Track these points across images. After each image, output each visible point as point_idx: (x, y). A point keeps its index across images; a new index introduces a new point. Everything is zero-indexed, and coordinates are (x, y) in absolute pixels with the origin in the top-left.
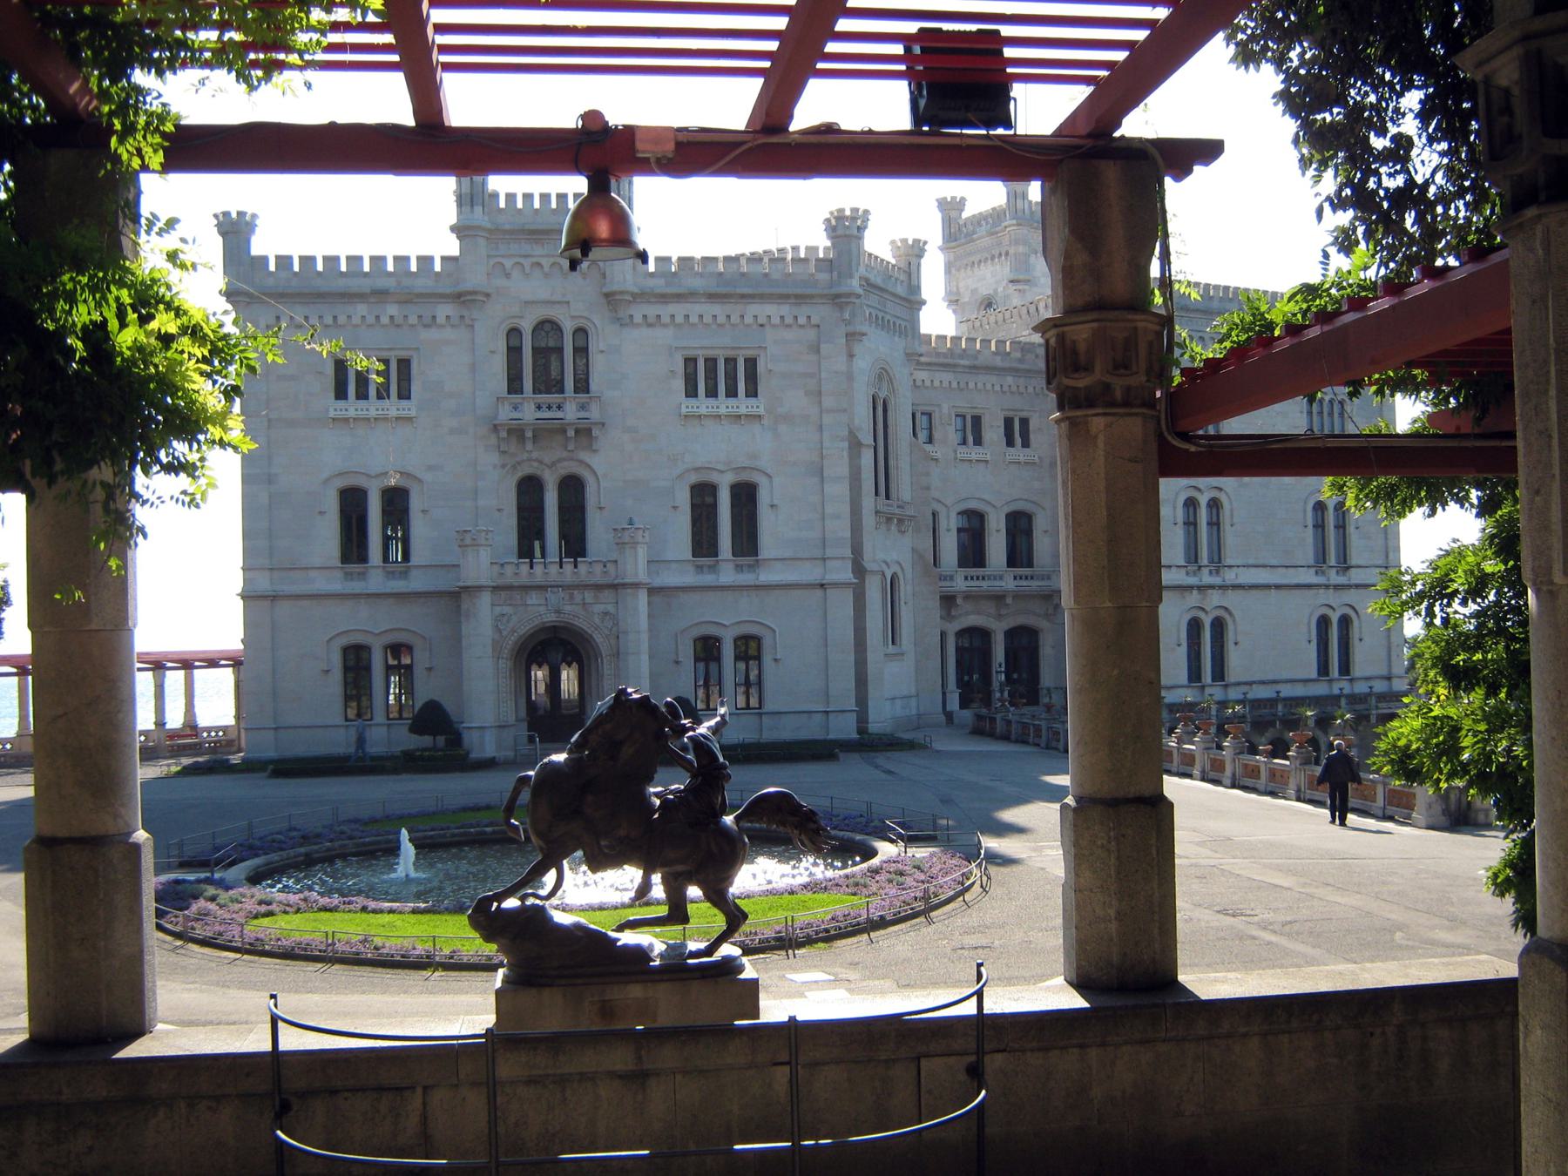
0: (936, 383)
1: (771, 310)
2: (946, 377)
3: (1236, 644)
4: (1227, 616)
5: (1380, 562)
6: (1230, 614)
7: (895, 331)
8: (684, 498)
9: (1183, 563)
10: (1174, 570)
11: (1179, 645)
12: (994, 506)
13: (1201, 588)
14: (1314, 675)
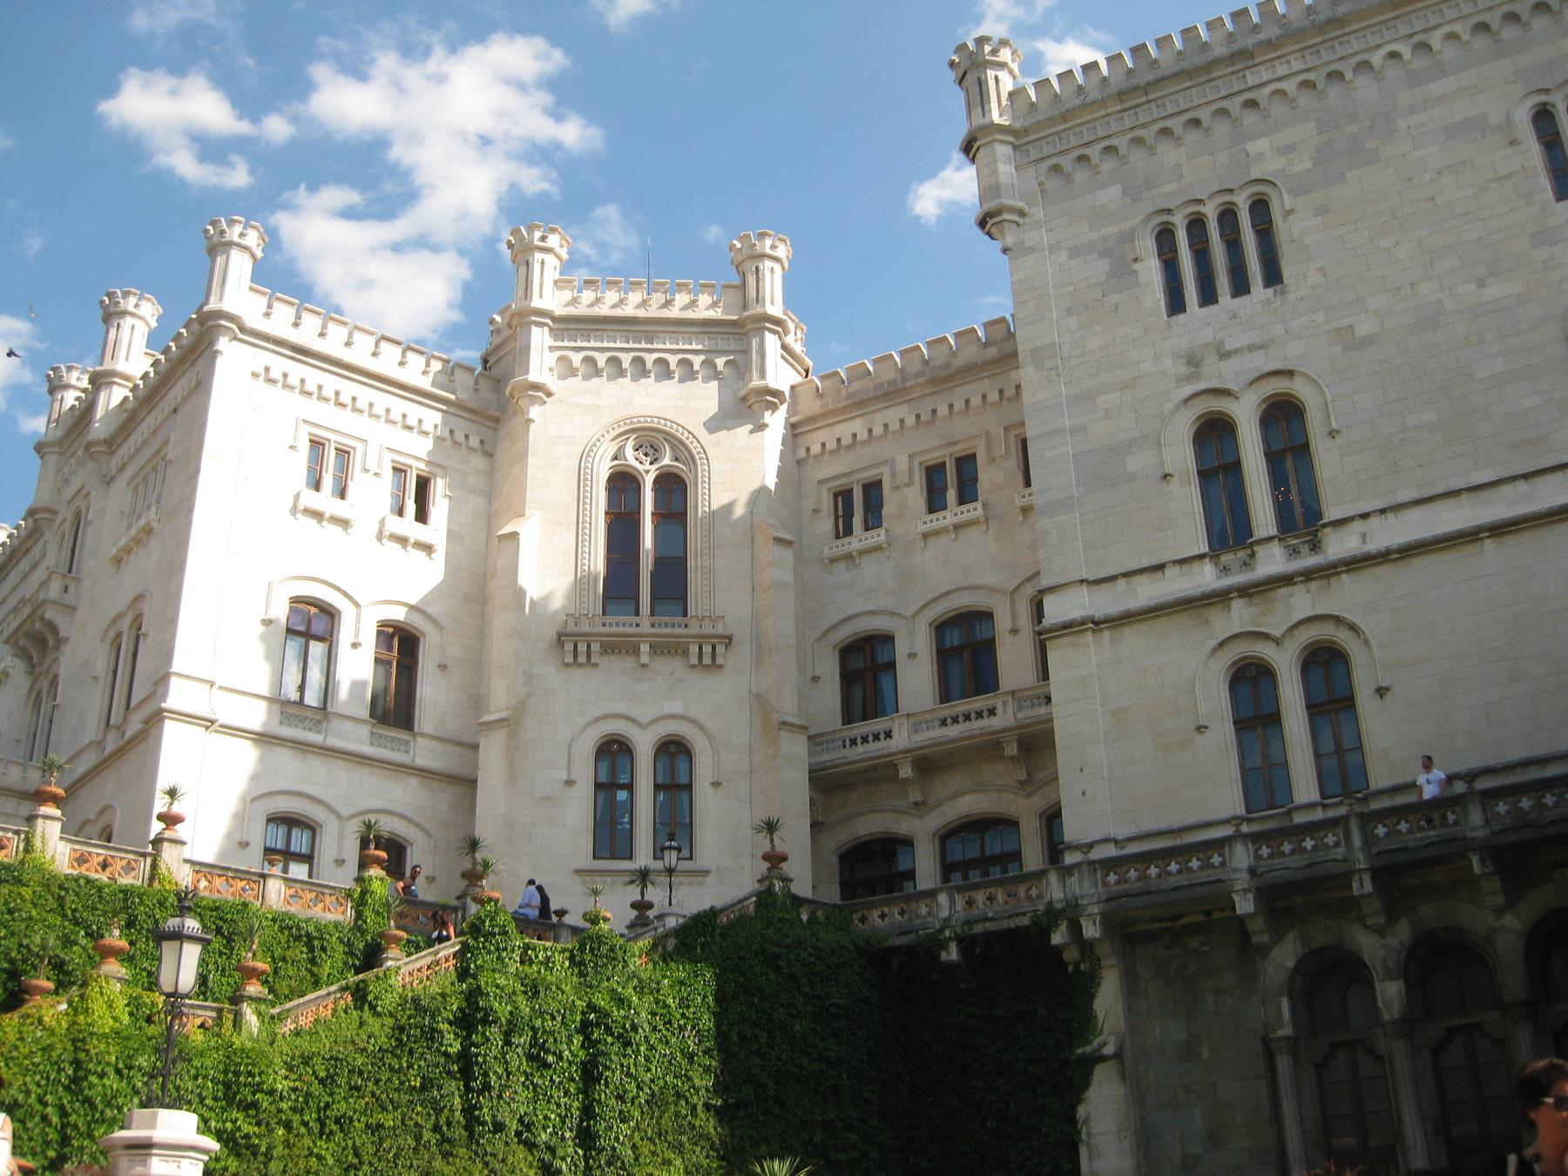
0: (878, 430)
2: (892, 416)
4: (1343, 637)
6: (1353, 628)
10: (1171, 572)
11: (1201, 729)
12: (1002, 593)
13: (1245, 591)
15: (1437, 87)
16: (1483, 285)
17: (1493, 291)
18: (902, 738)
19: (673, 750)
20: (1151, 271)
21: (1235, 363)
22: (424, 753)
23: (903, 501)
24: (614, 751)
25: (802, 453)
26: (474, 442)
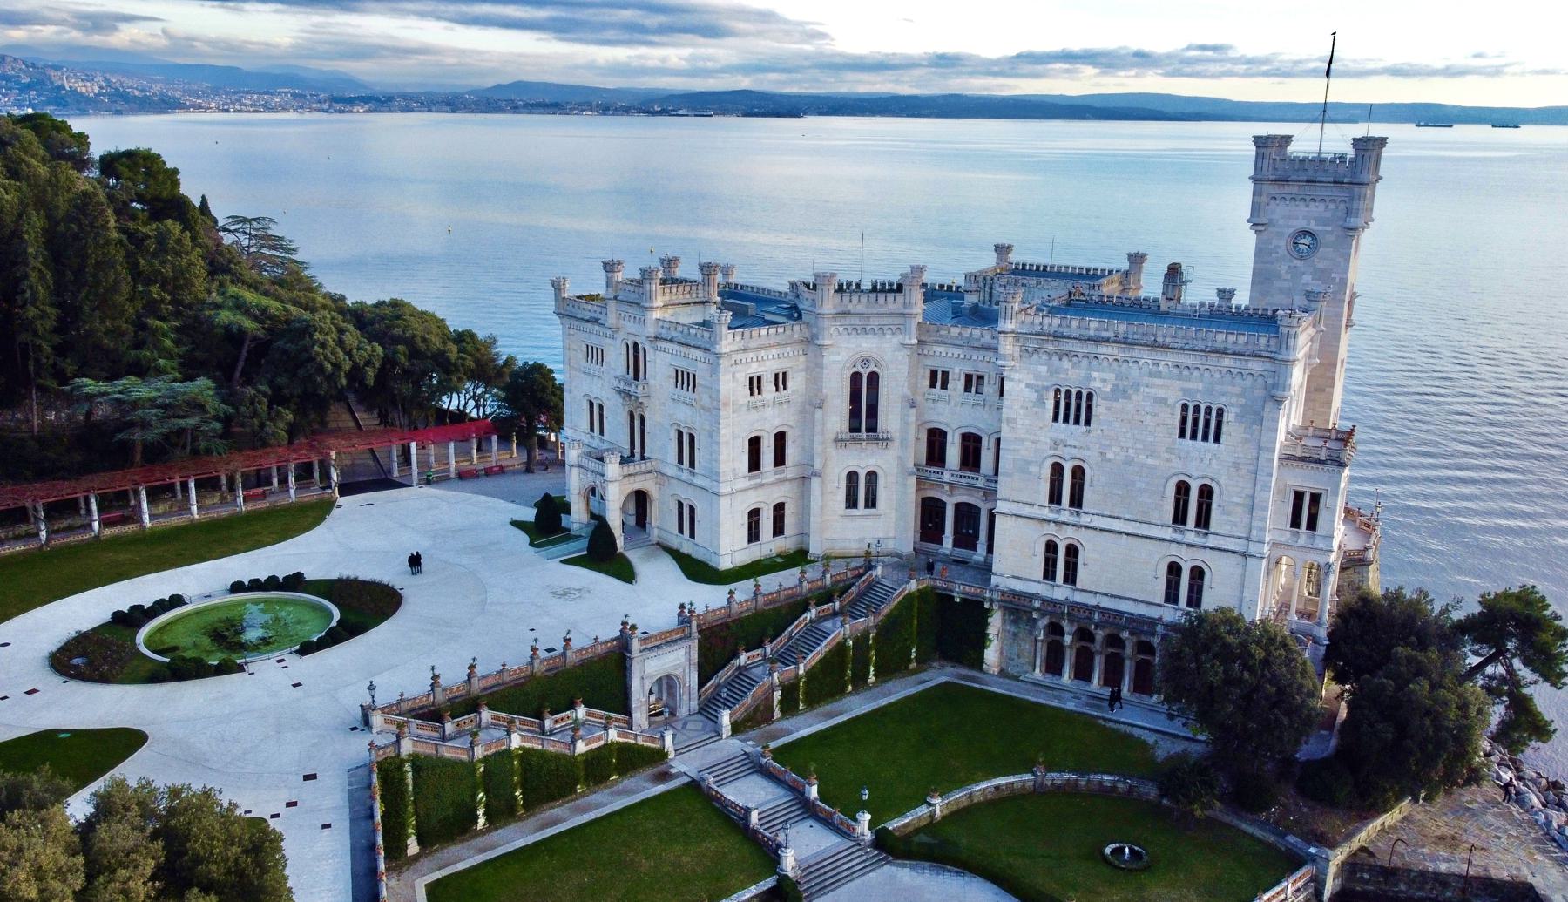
0: (950, 355)
2: (957, 351)
3: (1084, 565)
5: (1244, 535)
7: (884, 334)
8: (674, 436)
9: (1046, 504)
14: (1160, 598)
15: (1158, 381)
16: (1147, 457)
17: (1150, 461)
18: (947, 477)
19: (872, 476)
20: (1050, 404)
21: (1068, 448)
24: (852, 477)
25: (920, 352)
26: (801, 352)
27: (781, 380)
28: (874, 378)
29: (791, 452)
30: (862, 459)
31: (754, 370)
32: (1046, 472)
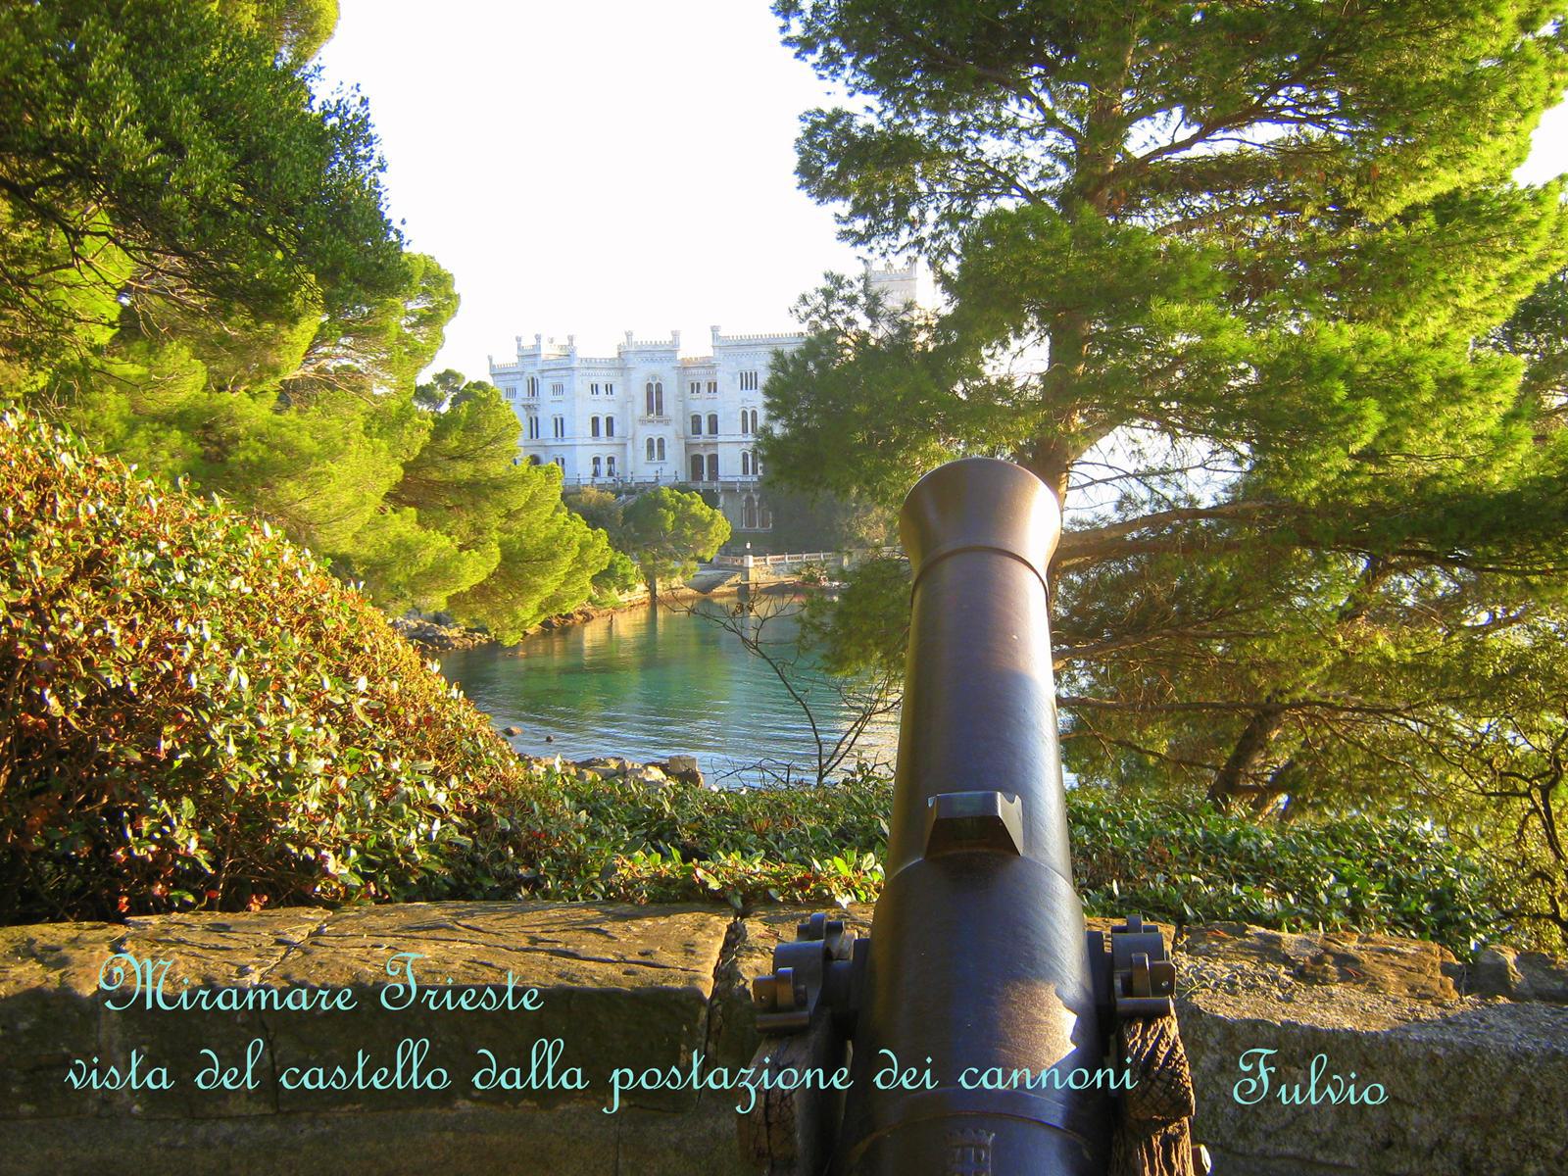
1: (564, 372)
2: (703, 371)
19: (661, 441)
22: (616, 440)
23: (704, 388)
24: (650, 441)
27: (609, 389)
28: (659, 386)
29: (616, 428)
30: (656, 432)
31: (594, 380)
32: (740, 417)
